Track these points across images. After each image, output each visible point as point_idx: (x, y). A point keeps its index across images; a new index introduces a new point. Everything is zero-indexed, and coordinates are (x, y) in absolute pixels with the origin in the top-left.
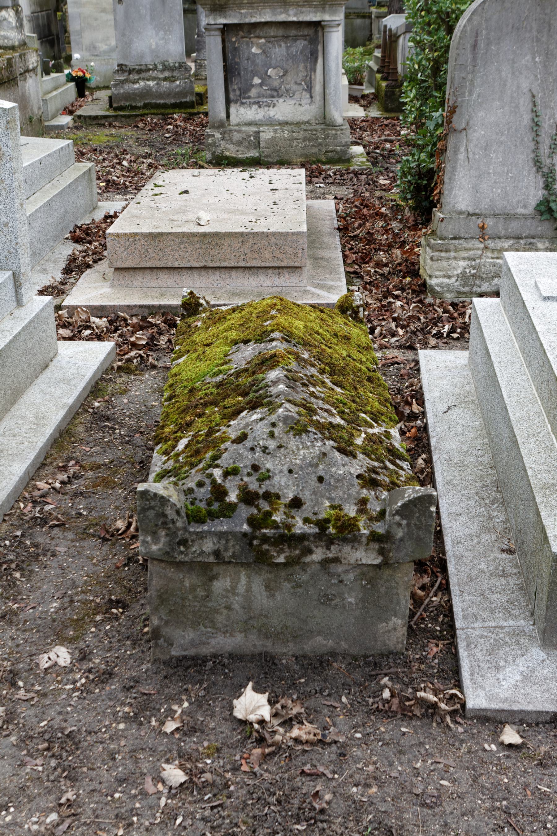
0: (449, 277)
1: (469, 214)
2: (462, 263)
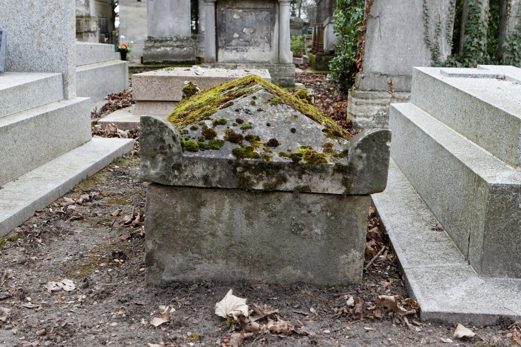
0: (368, 117)
1: (381, 75)
2: (377, 108)
